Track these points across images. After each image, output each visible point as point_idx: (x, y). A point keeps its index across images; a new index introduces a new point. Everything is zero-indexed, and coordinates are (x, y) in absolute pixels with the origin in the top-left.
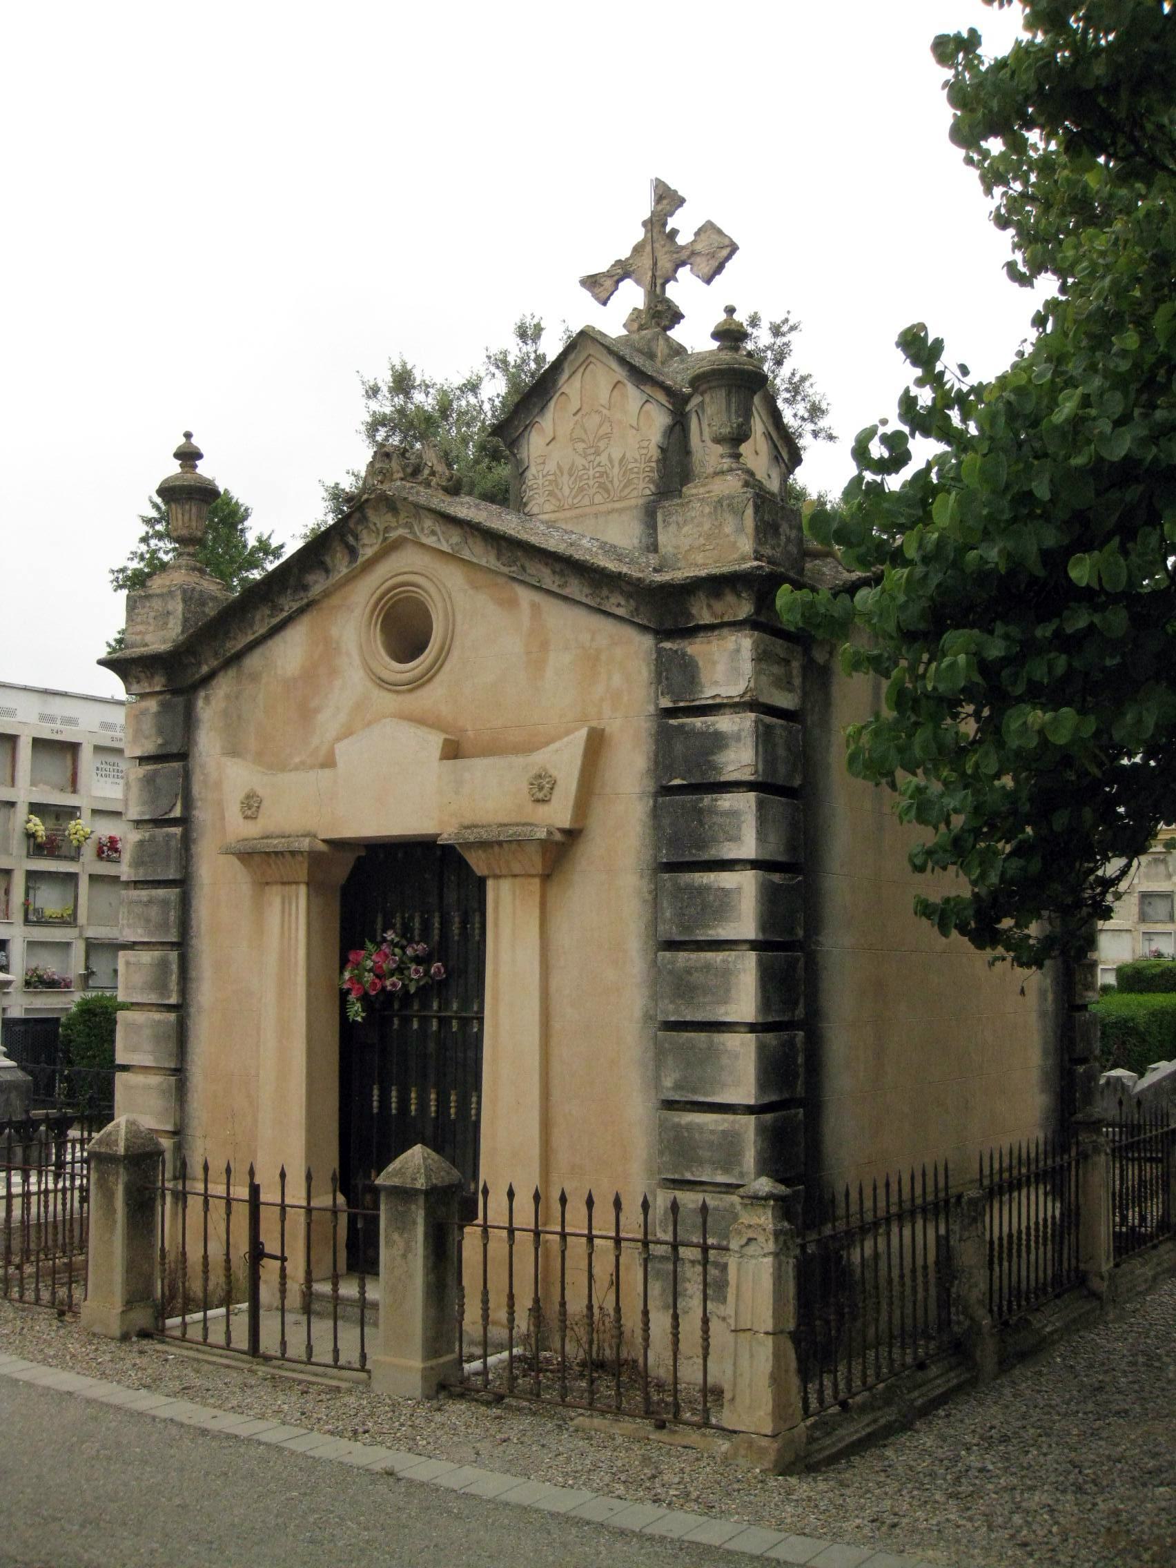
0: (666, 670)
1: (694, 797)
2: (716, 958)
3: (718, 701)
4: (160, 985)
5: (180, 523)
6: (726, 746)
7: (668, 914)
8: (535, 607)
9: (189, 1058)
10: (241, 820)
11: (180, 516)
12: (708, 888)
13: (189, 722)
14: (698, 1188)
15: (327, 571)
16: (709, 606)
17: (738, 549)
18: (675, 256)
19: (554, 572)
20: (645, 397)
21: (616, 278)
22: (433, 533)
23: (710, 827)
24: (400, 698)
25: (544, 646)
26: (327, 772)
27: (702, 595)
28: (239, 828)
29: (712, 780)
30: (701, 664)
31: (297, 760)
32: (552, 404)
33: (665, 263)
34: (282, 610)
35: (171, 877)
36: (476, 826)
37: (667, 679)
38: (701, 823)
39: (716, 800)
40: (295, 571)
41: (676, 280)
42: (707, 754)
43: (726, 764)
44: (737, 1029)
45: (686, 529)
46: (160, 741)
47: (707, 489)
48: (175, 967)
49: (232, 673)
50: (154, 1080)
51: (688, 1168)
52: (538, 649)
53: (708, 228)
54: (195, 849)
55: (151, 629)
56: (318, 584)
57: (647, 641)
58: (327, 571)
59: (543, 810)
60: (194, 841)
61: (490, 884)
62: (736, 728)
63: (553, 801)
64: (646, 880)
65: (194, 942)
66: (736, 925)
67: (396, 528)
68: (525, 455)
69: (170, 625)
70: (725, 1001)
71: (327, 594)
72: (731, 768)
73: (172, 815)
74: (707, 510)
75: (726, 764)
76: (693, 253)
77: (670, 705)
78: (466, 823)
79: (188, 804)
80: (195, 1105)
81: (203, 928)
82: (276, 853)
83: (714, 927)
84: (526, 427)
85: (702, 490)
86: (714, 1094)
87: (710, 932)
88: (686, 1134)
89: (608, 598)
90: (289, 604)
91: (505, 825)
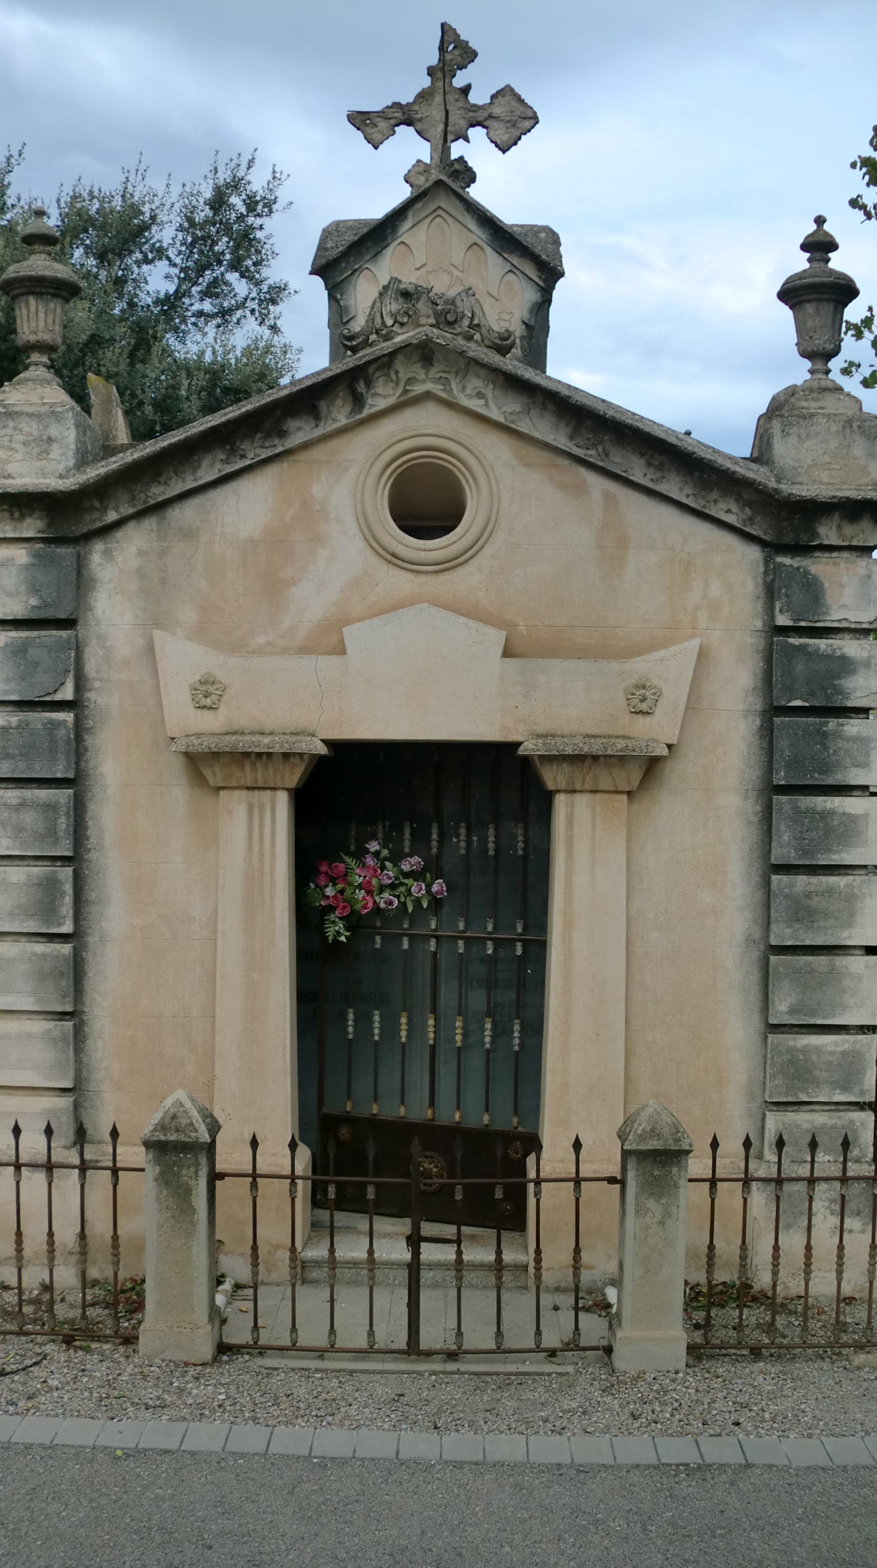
0: (786, 587)
1: (818, 720)
2: (840, 881)
3: (844, 625)
4: (47, 908)
5: (42, 324)
6: (853, 672)
7: (786, 838)
8: (608, 497)
9: (87, 998)
10: (191, 710)
11: (41, 315)
12: (832, 813)
13: (81, 582)
14: (804, 1108)
15: (317, 417)
16: (839, 527)
17: (869, 473)
18: (471, 114)
19: (649, 465)
20: (508, 267)
21: (392, 122)
22: (480, 395)
23: (835, 752)
24: (422, 579)
25: (623, 542)
26: (335, 660)
27: (836, 516)
28: (184, 718)
29: (838, 704)
30: (826, 585)
31: (261, 640)
32: (388, 252)
33: (457, 119)
34: (243, 457)
35: (59, 775)
36: (553, 736)
37: (787, 596)
38: (826, 748)
39: (843, 725)
40: (278, 413)
41: (467, 140)
42: (833, 677)
43: (855, 689)
44: (851, 952)
45: (808, 444)
46: (34, 601)
47: (819, 404)
48: (69, 888)
49: (150, 523)
50: (40, 1026)
51: (805, 1090)
52: (614, 547)
53: (507, 93)
54: (89, 741)
55: (19, 456)
56: (301, 431)
57: (754, 553)
58: (317, 417)
59: (642, 722)
60: (89, 730)
61: (560, 801)
62: (865, 655)
63: (658, 713)
64: (751, 801)
65: (93, 855)
66: (862, 850)
67: (424, 381)
68: (352, 302)
69: (52, 456)
70: (849, 923)
71: (306, 446)
72: (858, 694)
73: (58, 697)
74: (834, 428)
75: (855, 689)
76: (490, 116)
77: (790, 623)
78: (540, 730)
79: (80, 685)
80: (100, 1054)
81: (108, 839)
82: (259, 755)
83: (838, 852)
84: (355, 271)
85: (813, 404)
86: (834, 1016)
87: (833, 857)
88: (802, 1057)
89: (716, 501)
90: (254, 452)
91: (595, 736)
